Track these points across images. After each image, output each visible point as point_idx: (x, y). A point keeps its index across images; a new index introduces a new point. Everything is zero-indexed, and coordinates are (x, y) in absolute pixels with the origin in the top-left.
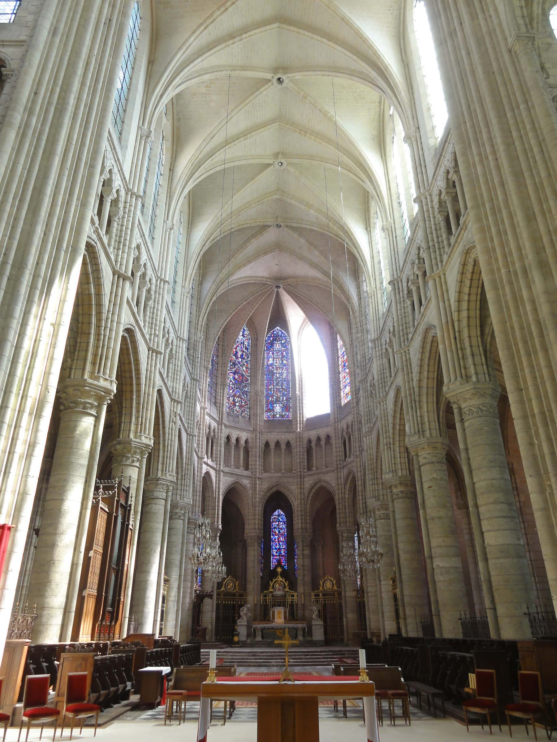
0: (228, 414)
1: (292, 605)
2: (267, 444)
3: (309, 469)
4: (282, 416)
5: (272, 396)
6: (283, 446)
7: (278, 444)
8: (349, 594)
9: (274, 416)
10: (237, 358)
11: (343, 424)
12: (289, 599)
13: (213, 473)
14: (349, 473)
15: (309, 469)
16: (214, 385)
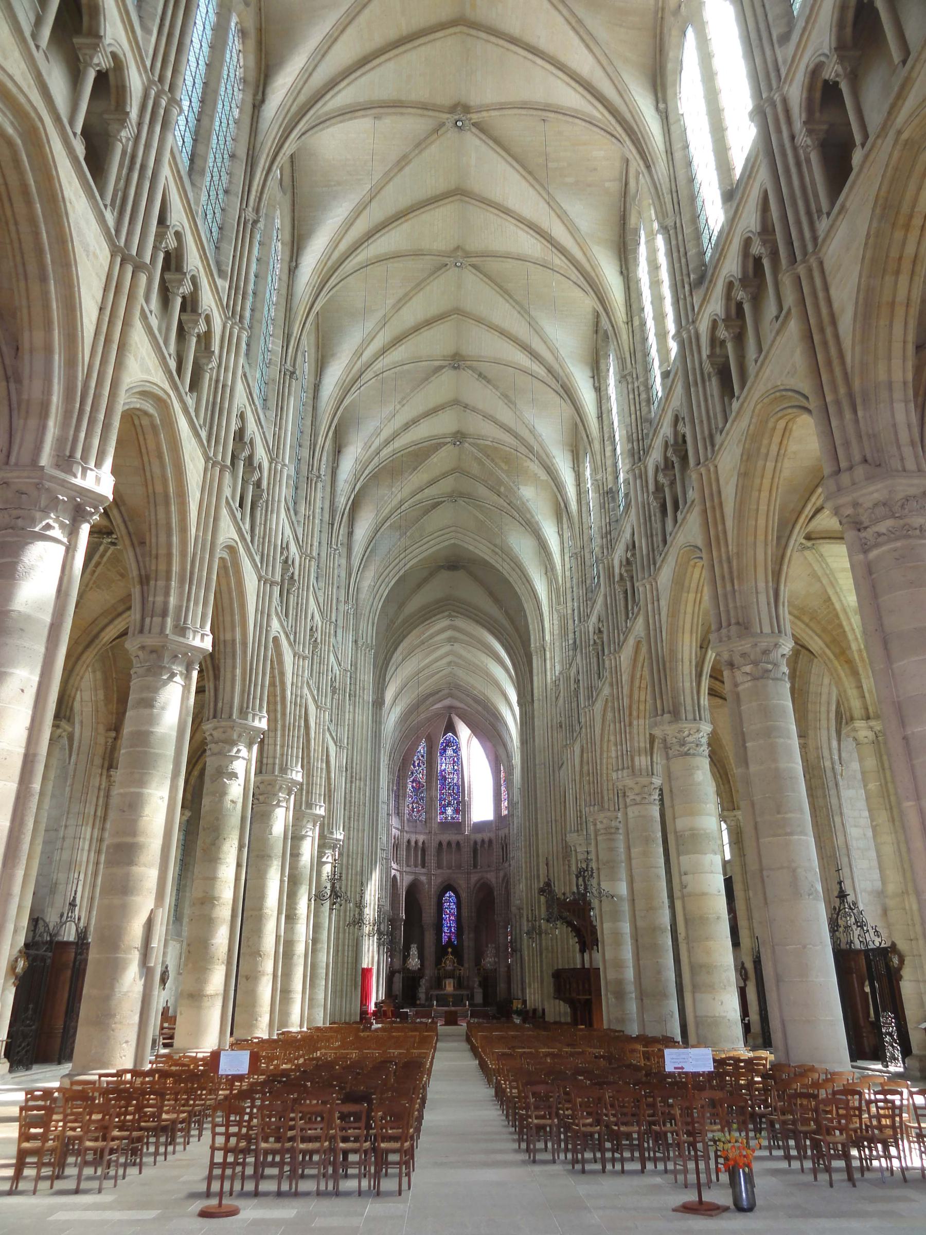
0: (408, 820)
1: (459, 978)
2: (440, 844)
3: (475, 866)
4: (453, 818)
5: (445, 800)
6: (454, 845)
7: (449, 844)
8: (503, 969)
9: (446, 818)
10: (414, 766)
11: (502, 833)
12: (457, 972)
13: (398, 875)
14: (505, 876)
15: (475, 866)
16: (397, 797)
